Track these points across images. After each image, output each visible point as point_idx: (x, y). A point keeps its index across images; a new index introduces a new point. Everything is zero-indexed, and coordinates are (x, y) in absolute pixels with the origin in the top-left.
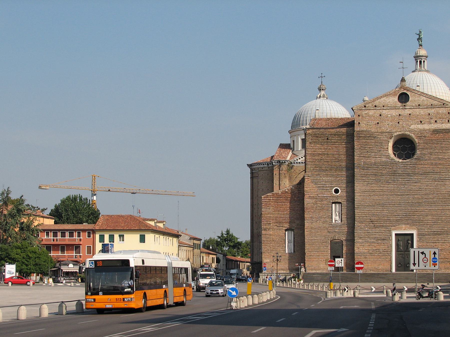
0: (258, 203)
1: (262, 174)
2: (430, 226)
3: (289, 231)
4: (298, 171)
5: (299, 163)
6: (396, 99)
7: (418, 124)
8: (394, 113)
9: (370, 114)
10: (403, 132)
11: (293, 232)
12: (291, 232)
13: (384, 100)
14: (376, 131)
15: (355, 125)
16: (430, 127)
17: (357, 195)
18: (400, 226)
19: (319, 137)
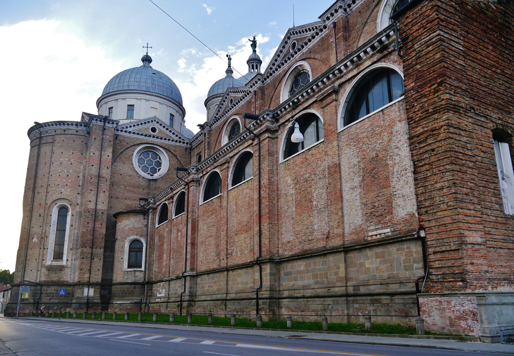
0: (49, 184)
1: (63, 139)
4: (126, 144)
5: (130, 132)
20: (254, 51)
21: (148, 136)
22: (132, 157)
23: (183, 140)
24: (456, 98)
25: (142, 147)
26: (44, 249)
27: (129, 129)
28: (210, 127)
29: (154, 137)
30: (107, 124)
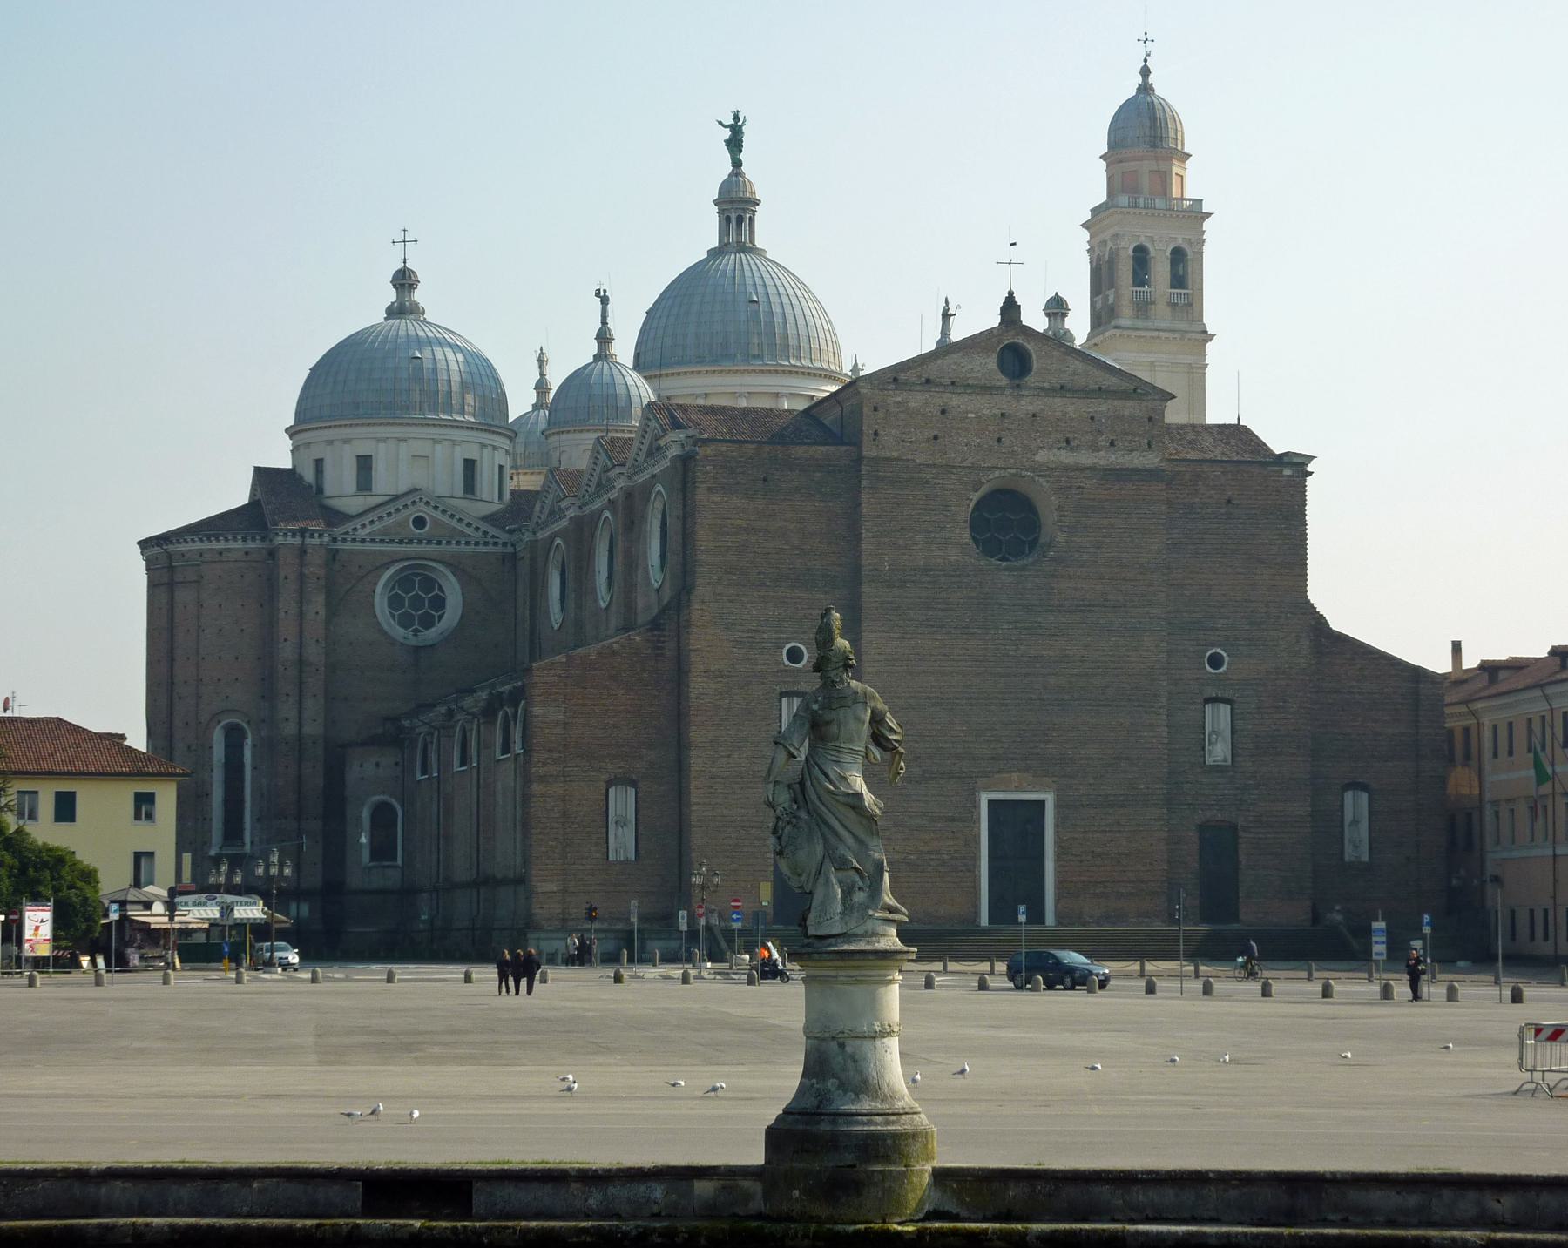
2: (1095, 778)
3: (620, 787)
5: (363, 541)
6: (991, 362)
7: (1059, 449)
8: (985, 406)
9: (912, 405)
10: (1013, 471)
11: (631, 791)
12: (626, 791)
13: (955, 363)
14: (931, 462)
15: (865, 438)
16: (1095, 461)
17: (870, 670)
18: (1004, 775)
19: (738, 470)
20: (737, 164)
21: (406, 543)
22: (373, 597)
23: (493, 537)
24: (546, 769)
25: (392, 570)
26: (205, 819)
27: (362, 533)
28: (534, 533)
29: (420, 542)
30: (308, 541)
